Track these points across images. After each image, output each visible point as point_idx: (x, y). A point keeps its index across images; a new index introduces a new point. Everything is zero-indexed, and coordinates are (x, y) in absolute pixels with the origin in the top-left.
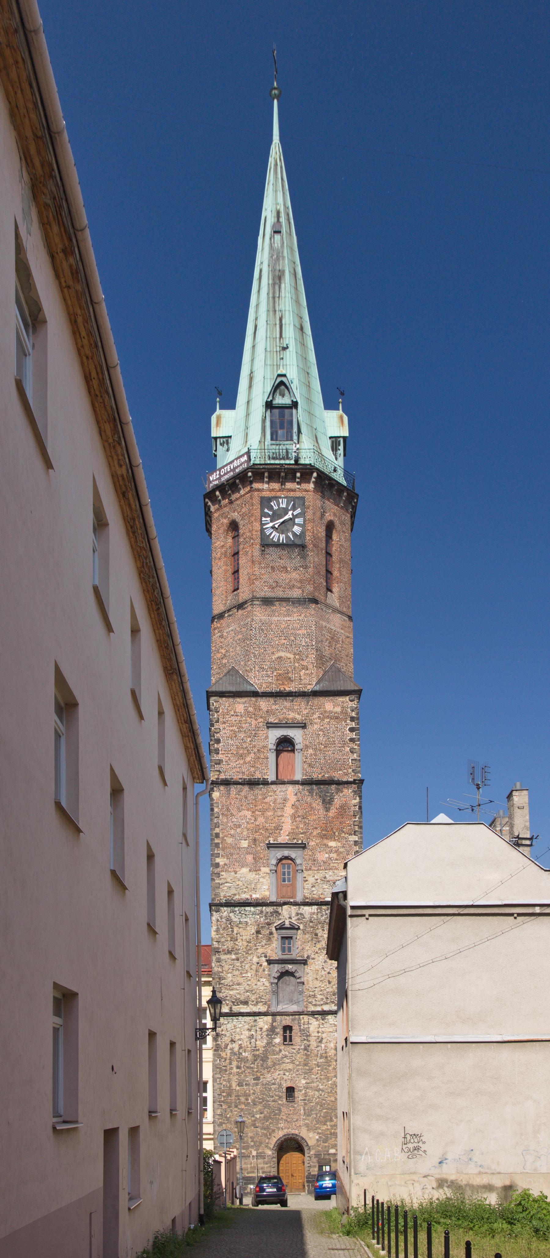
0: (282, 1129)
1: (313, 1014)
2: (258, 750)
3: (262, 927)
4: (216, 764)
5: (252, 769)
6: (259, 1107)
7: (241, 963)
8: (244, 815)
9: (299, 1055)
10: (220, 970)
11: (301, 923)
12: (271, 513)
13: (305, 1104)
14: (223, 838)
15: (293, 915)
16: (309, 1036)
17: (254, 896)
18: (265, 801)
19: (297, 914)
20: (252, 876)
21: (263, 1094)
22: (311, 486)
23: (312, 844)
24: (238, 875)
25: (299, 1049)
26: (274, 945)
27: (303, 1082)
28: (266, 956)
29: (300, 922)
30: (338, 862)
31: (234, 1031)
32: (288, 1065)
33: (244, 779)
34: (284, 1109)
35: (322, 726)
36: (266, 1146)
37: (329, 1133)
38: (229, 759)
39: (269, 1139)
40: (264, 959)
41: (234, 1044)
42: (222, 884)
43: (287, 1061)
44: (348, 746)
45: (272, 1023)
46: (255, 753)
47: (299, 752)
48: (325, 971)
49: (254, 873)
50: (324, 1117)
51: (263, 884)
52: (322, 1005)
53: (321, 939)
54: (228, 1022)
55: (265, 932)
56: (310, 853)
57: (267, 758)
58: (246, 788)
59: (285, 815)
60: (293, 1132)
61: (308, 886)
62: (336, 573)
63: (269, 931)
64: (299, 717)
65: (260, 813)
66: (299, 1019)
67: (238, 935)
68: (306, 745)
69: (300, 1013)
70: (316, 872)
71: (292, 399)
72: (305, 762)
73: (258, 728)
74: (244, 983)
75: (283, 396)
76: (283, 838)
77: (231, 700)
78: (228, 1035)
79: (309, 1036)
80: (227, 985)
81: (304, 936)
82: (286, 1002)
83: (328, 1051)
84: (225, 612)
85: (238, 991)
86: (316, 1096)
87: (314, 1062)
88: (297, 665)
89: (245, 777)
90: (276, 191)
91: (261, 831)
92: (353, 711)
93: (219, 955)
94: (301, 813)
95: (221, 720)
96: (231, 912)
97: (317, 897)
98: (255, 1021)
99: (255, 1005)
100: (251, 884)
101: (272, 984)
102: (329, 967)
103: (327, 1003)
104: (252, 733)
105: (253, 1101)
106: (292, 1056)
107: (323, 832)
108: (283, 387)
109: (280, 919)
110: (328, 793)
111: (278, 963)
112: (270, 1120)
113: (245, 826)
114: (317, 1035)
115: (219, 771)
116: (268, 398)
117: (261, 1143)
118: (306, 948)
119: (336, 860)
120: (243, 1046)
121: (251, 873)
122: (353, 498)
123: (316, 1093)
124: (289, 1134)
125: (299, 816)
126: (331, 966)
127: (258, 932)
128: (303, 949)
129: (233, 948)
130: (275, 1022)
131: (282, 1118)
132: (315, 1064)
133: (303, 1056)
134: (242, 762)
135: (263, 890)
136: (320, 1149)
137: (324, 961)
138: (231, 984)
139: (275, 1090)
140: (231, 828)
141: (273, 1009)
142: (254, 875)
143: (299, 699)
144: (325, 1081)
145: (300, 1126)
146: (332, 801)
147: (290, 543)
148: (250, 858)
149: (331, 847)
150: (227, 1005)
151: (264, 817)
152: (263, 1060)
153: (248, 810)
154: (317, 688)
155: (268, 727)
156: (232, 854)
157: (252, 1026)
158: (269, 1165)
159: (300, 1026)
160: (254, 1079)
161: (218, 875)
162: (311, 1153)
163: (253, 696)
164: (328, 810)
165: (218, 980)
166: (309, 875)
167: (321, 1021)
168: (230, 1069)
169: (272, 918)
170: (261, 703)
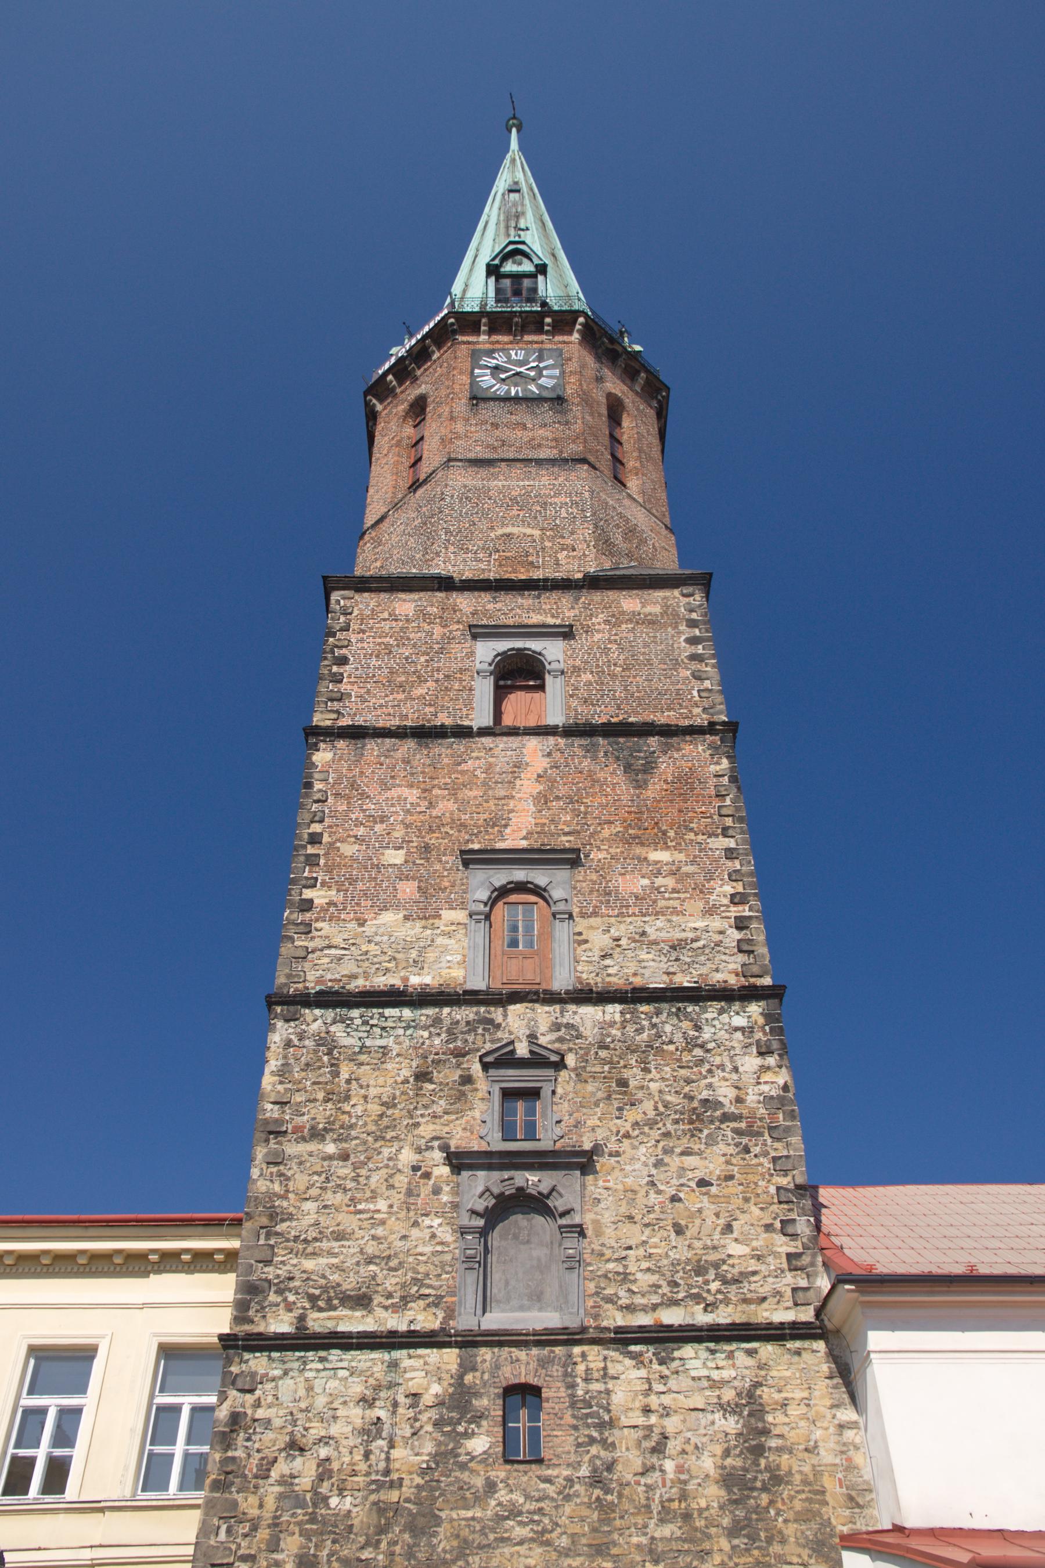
2: (447, 677)
3: (437, 1063)
7: (355, 1167)
8: (399, 797)
9: (568, 1509)
10: (277, 1188)
11: (570, 1050)
14: (331, 844)
15: (543, 1027)
16: (611, 1424)
17: (415, 980)
18: (459, 768)
20: (413, 930)
22: (576, 336)
24: (369, 929)
25: (569, 1480)
26: (477, 1114)
29: (565, 1047)
30: (682, 896)
32: (522, 1549)
35: (616, 635)
38: (368, 692)
40: (438, 1156)
41: (299, 1460)
42: (313, 952)
43: (520, 1532)
44: (688, 669)
45: (461, 1377)
46: (437, 681)
47: (555, 677)
48: (659, 1192)
49: (419, 924)
51: (445, 950)
52: (655, 1307)
53: (640, 1095)
54: (286, 1373)
56: (594, 876)
57: (471, 690)
58: (411, 744)
62: (631, 463)
63: (459, 1072)
65: (446, 792)
68: (574, 667)
70: (613, 920)
72: (571, 696)
74: (359, 1233)
76: (513, 839)
77: (384, 596)
78: (277, 1422)
79: (611, 1424)
80: (296, 1238)
81: (579, 1086)
82: (515, 1303)
83: (691, 1487)
85: (334, 1261)
87: (635, 1540)
88: (548, 544)
89: (409, 723)
91: (447, 829)
92: (691, 611)
93: (280, 1143)
94: (562, 790)
96: (334, 1022)
97: (622, 982)
98: (394, 1365)
99: (395, 1308)
100: (405, 950)
101: (463, 1231)
102: (675, 1182)
103: (676, 1303)
104: (431, 648)
106: (540, 1511)
110: (639, 751)
111: (490, 1167)
113: (400, 818)
114: (641, 1421)
115: (338, 712)
116: (493, 259)
118: (589, 1123)
119: (674, 891)
120: (335, 1466)
121: (409, 924)
122: (658, 391)
125: (558, 798)
126: (680, 1177)
127: (422, 1076)
128: (577, 1124)
130: (474, 1369)
132: (639, 1546)
133: (586, 1512)
134: (401, 696)
135: (444, 965)
137: (653, 1160)
138: (312, 1234)
140: (358, 823)
141: (466, 1321)
143: (555, 595)
146: (653, 768)
147: (530, 396)
148: (408, 889)
149: (657, 862)
150: (289, 1307)
151: (456, 799)
152: (412, 1528)
155: (475, 637)
156: (353, 881)
157: (377, 1388)
159: (573, 1386)
163: (439, 590)
164: (641, 785)
165: (264, 1221)
166: (591, 928)
167: (656, 1366)
169: (470, 1038)
170: (458, 601)
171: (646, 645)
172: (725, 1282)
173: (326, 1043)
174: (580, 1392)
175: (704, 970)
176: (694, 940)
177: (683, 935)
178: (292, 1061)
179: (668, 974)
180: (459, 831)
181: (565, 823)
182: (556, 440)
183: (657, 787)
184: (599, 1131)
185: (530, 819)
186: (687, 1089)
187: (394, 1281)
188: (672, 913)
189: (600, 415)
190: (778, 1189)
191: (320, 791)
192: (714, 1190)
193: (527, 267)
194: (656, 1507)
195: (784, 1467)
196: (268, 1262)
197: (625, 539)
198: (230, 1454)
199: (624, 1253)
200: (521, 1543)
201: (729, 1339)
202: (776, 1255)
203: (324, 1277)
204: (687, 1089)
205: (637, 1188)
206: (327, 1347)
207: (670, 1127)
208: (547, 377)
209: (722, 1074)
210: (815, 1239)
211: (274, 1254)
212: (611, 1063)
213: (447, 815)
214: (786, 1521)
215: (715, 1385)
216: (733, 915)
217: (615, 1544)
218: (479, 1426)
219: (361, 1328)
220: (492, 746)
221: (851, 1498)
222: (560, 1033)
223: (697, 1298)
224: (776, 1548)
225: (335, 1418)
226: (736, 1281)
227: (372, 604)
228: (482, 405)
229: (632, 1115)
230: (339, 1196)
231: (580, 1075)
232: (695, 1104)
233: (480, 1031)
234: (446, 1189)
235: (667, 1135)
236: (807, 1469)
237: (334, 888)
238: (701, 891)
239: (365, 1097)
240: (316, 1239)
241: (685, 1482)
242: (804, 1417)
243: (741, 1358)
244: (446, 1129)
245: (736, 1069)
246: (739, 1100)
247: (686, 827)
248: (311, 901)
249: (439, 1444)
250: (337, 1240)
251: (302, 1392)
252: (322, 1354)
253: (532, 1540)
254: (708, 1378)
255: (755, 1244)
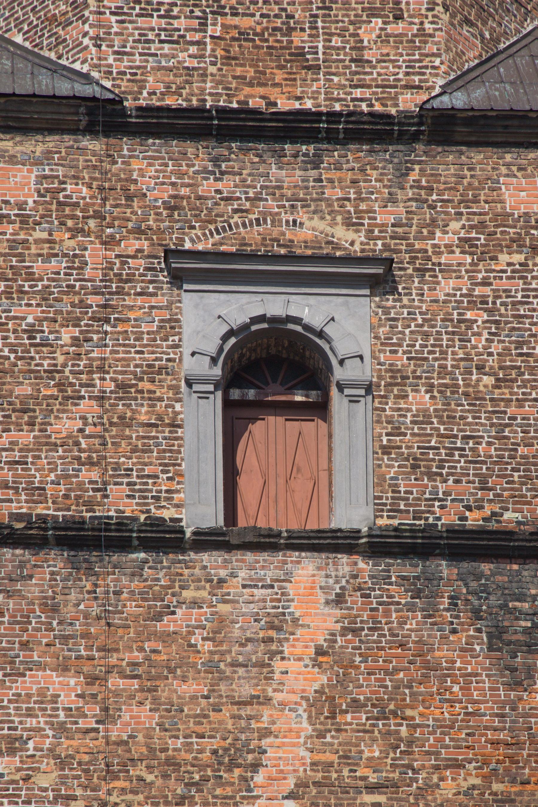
8: (42, 693)
65: (135, 684)
91: (140, 770)
151: (155, 700)
180: (166, 776)
181: (371, 763)
185: (303, 753)
213: (140, 738)
220: (223, 573)
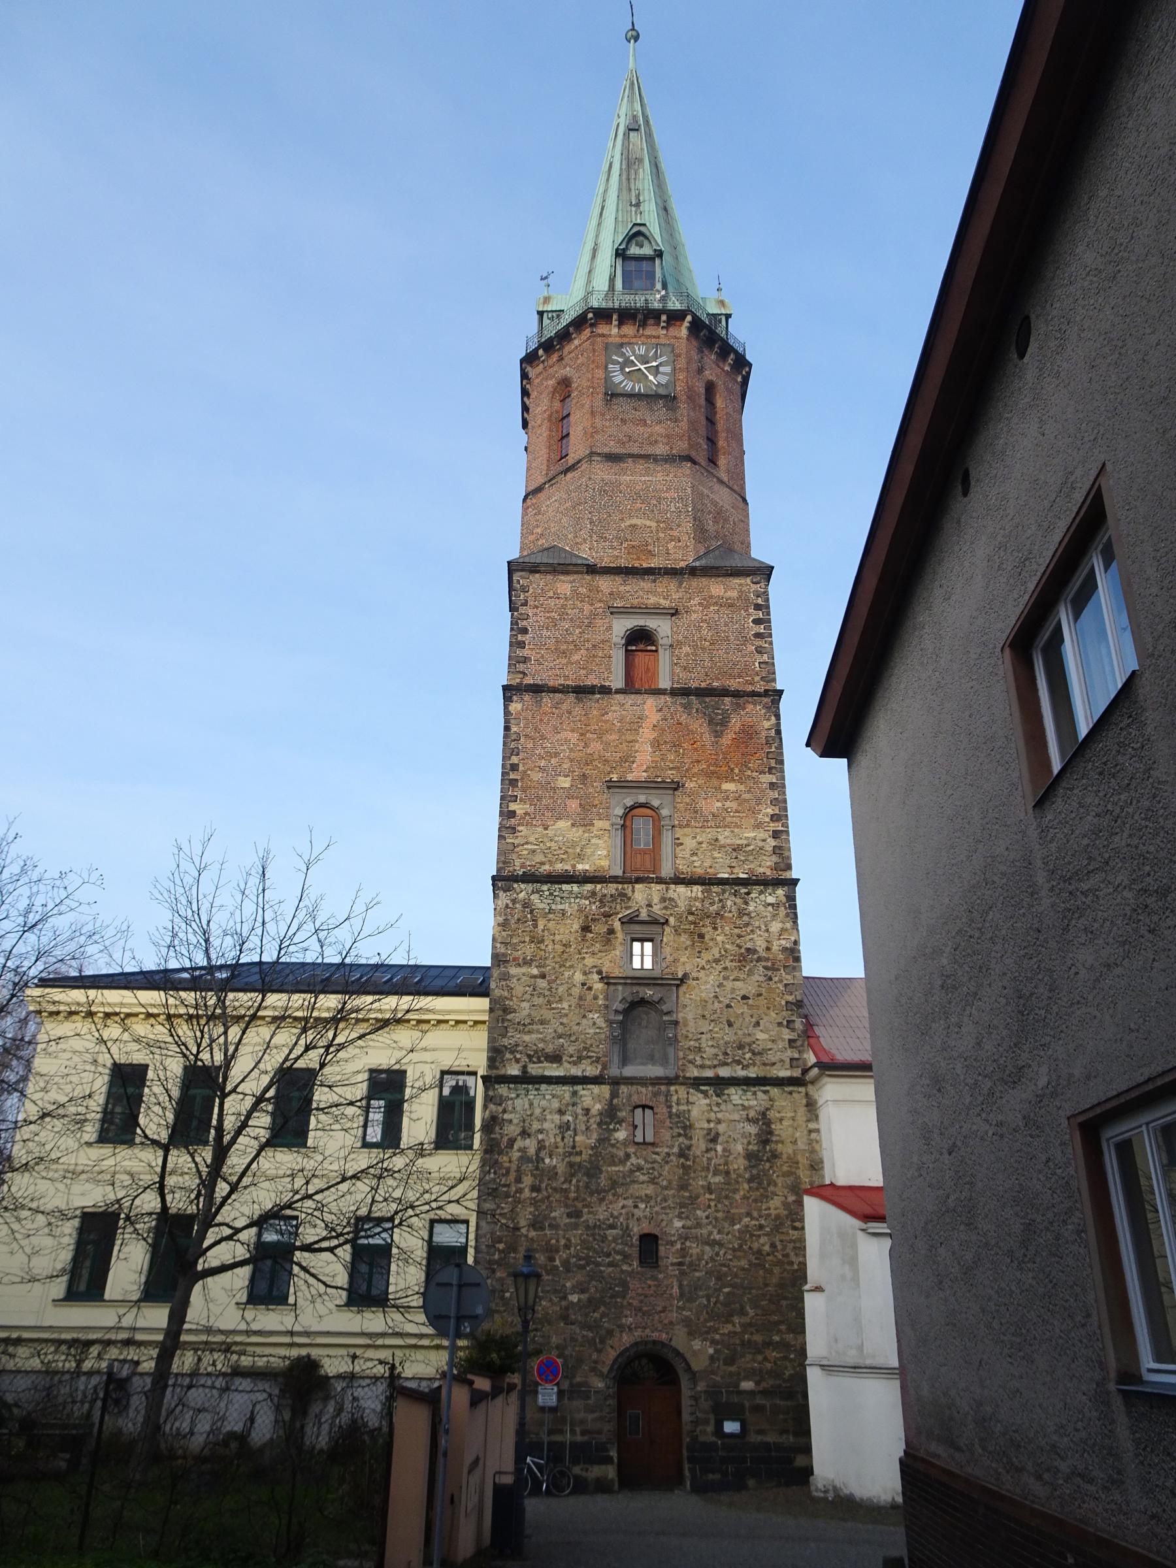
0: (630, 1329)
1: (697, 1083)
2: (594, 646)
3: (593, 920)
4: (519, 662)
5: (583, 672)
6: (580, 1277)
8: (566, 738)
9: (667, 1168)
10: (506, 994)
11: (671, 915)
12: (620, 360)
13: (682, 1273)
14: (525, 772)
15: (656, 900)
16: (691, 1127)
17: (580, 867)
19: (663, 900)
20: (576, 834)
21: (588, 1249)
23: (690, 785)
24: (550, 832)
25: (668, 1154)
26: (618, 953)
27: (678, 1224)
28: (600, 972)
30: (741, 815)
31: (529, 1113)
33: (568, 685)
34: (634, 1284)
36: (593, 1370)
37: (738, 1342)
39: (600, 1351)
40: (596, 977)
41: (528, 1141)
42: (518, 846)
43: (642, 1178)
44: (753, 645)
45: (611, 1100)
46: (588, 649)
48: (720, 1002)
49: (581, 829)
50: (726, 1305)
51: (597, 846)
52: (715, 1067)
53: (711, 944)
54: (518, 1096)
55: (600, 928)
56: (687, 800)
59: (640, 740)
60: (655, 1335)
61: (684, 853)
64: (665, 603)
66: (668, 1094)
67: (546, 933)
68: (678, 641)
69: (670, 1081)
71: (655, 247)
72: (676, 664)
73: (593, 615)
74: (553, 1021)
75: (641, 246)
76: (637, 773)
77: (549, 577)
78: (515, 1121)
80: (519, 1023)
84: (545, 484)
85: (541, 1036)
86: (706, 1257)
87: (701, 1183)
88: (662, 535)
90: (632, 102)
92: (758, 596)
94: (668, 737)
95: (530, 603)
96: (533, 892)
97: (702, 871)
98: (575, 1093)
99: (575, 1063)
100: (573, 847)
101: (610, 1023)
102: (729, 996)
103: (726, 1064)
105: (566, 1263)
106: (653, 1168)
107: (711, 768)
108: (641, 238)
109: (627, 908)
112: (602, 1308)
114: (706, 1125)
115: (524, 673)
117: (580, 1361)
120: (547, 1144)
121: (574, 829)
123: (707, 1248)
124: (646, 1343)
126: (732, 993)
127: (586, 929)
129: (536, 956)
130: (618, 1097)
131: (630, 1304)
132: (702, 1186)
133: (676, 1170)
134: (564, 661)
135: (596, 857)
136: (718, 1379)
137: (717, 983)
138: (527, 1021)
139: (615, 1240)
141: (614, 1071)
142: (580, 832)
143: (665, 580)
144: (726, 1225)
145: (671, 1323)
147: (650, 393)
148: (573, 805)
149: (726, 791)
150: (517, 1061)
152: (588, 1174)
153: (573, 731)
154: (697, 564)
156: (539, 799)
157: (567, 1105)
158: (597, 1415)
159: (670, 1107)
160: (569, 1215)
161: (513, 830)
162: (699, 1388)
164: (718, 735)
165: (501, 1013)
167: (715, 1098)
168: (517, 1192)
169: (613, 905)
171: (726, 625)
172: (754, 1054)
173: (526, 904)
174: (674, 1110)
175: (752, 866)
176: (748, 845)
177: (740, 842)
178: (510, 917)
179: (730, 867)
181: (671, 761)
182: (667, 436)
183: (729, 736)
184: (687, 965)
186: (738, 941)
187: (573, 1048)
188: (734, 827)
189: (700, 407)
190: (787, 1002)
191: (515, 733)
192: (750, 1002)
193: (647, 251)
194: (712, 1168)
195: (779, 1150)
196: (504, 1036)
197: (716, 522)
198: (493, 1136)
199: (699, 1036)
200: (643, 1183)
201: (754, 1085)
202: (783, 1040)
203: (535, 1045)
204: (738, 941)
205: (707, 999)
206: (540, 1083)
207: (728, 964)
208: (663, 374)
209: (759, 933)
210: (805, 1032)
211: (507, 1032)
212: (695, 923)
214: (778, 1176)
215: (744, 1108)
216: (772, 829)
217: (690, 1185)
218: (621, 1126)
219: (557, 1074)
221: (812, 1166)
222: (666, 904)
223: (739, 1062)
224: (771, 1188)
225: (545, 1120)
226: (760, 1053)
227: (542, 583)
228: (615, 401)
229: (707, 956)
230: (541, 999)
231: (677, 932)
232: (743, 950)
233: (619, 901)
234: (601, 997)
235: (725, 968)
236: (790, 1151)
237: (528, 802)
238: (754, 812)
239: (553, 941)
240: (530, 1024)
241: (728, 1156)
242: (791, 1126)
243: (760, 1094)
244: (600, 961)
245: (767, 931)
246: (768, 949)
247: (746, 766)
248: (514, 812)
249: (600, 1134)
250: (541, 1024)
251: (527, 1106)
252: (537, 1086)
253: (649, 1182)
254: (742, 1105)
255: (772, 1033)
